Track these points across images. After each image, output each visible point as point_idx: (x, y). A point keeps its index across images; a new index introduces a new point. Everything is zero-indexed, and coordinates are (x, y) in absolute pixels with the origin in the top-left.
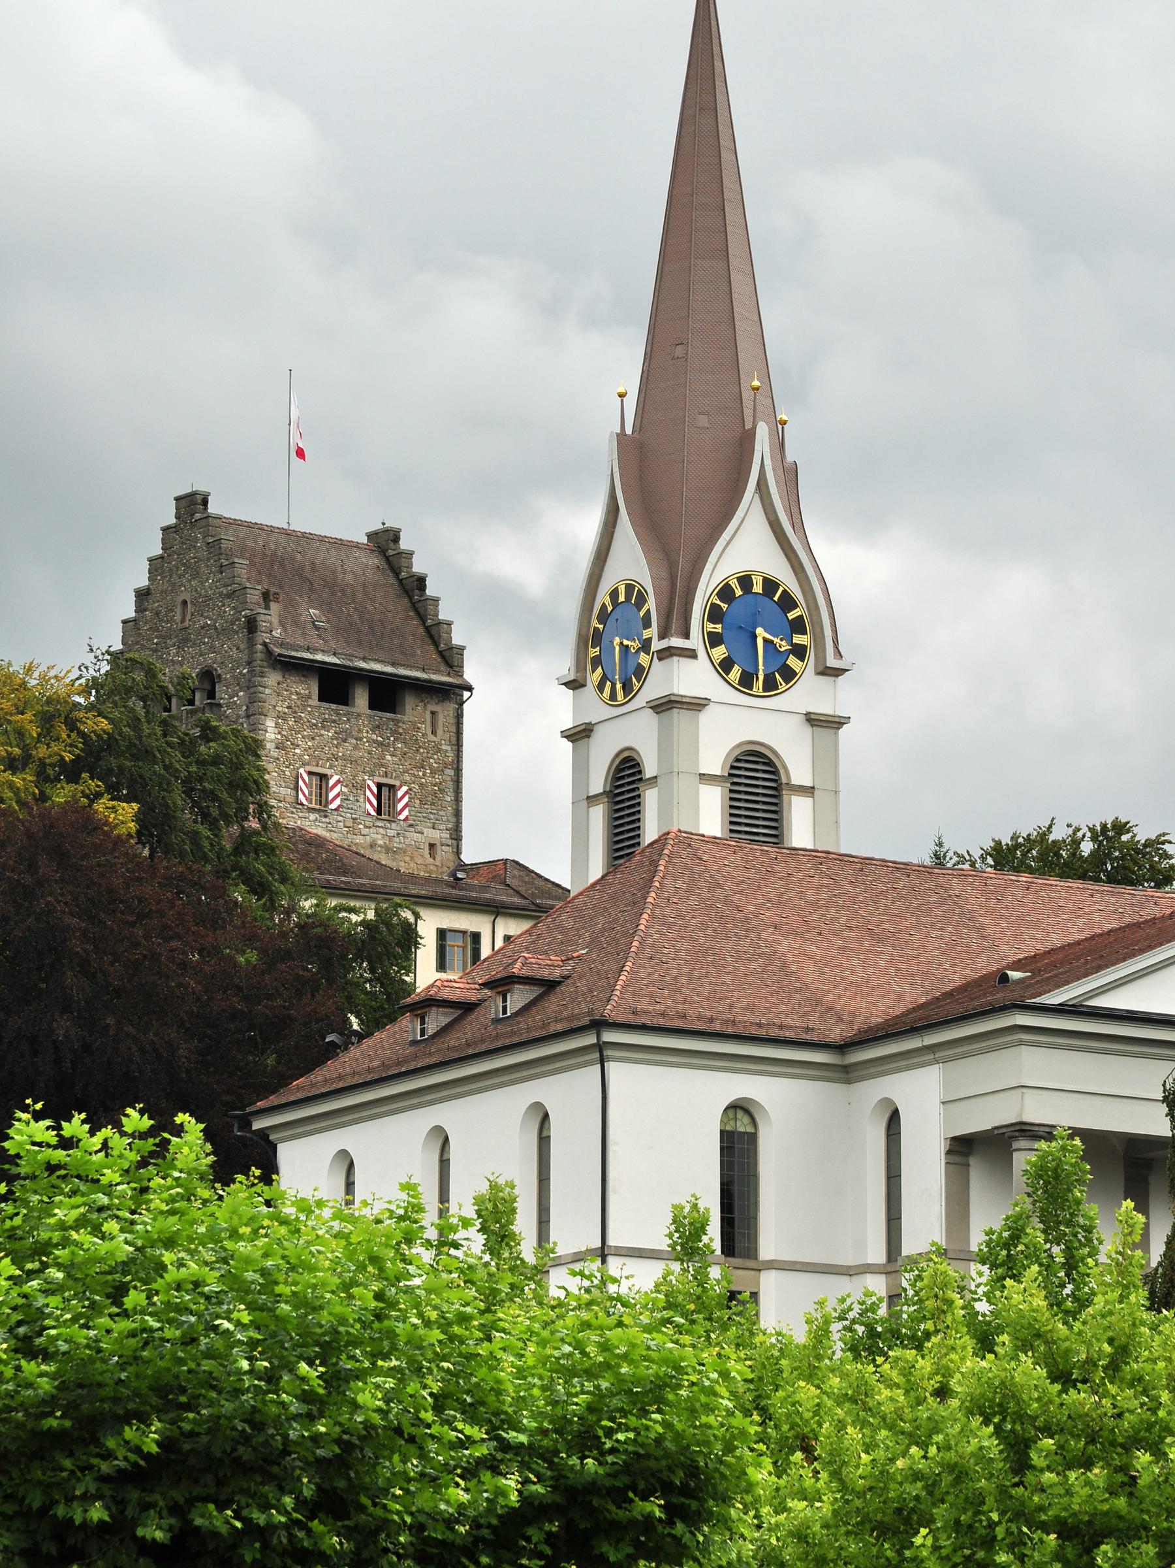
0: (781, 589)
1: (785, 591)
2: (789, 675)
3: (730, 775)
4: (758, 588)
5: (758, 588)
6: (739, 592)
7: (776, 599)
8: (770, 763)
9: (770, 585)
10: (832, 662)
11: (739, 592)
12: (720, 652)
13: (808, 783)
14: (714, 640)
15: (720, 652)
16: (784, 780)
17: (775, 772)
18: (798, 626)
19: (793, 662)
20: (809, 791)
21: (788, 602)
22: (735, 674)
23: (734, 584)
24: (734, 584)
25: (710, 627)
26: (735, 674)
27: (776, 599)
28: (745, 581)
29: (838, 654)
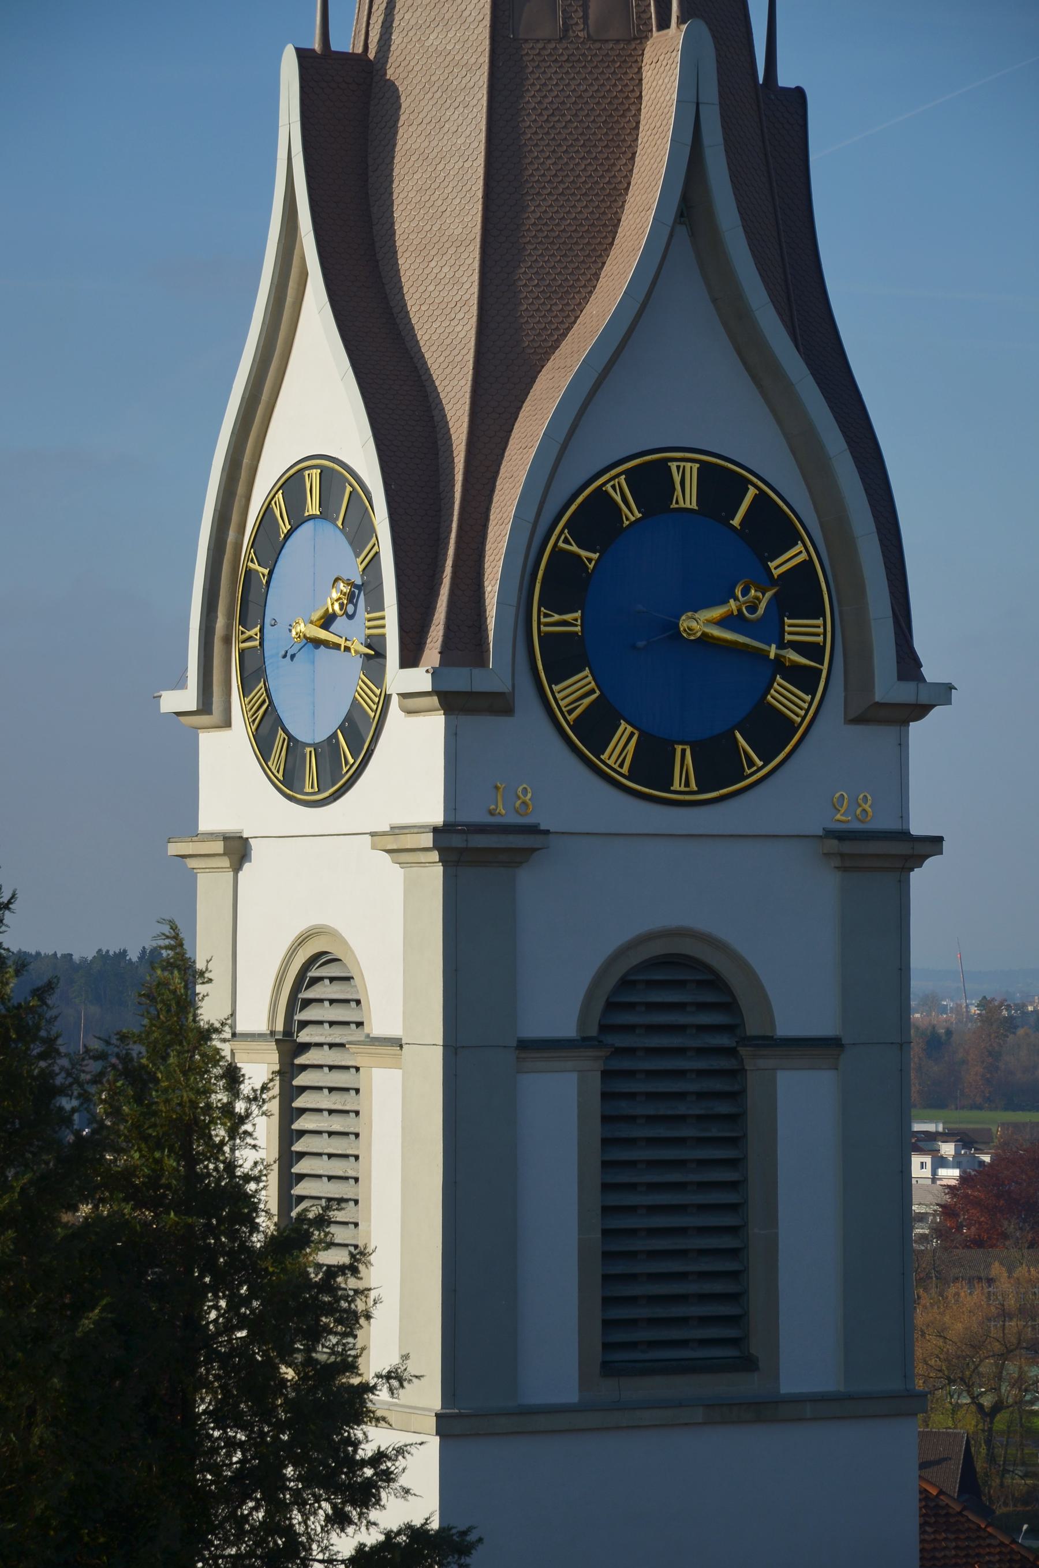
0: (752, 492)
1: (761, 498)
2: (774, 733)
3: (603, 1028)
4: (687, 498)
5: (687, 498)
6: (632, 514)
7: (736, 522)
8: (714, 981)
9: (721, 483)
10: (887, 687)
11: (632, 514)
12: (577, 691)
14: (561, 657)
15: (577, 691)
16: (753, 1029)
17: (731, 1006)
18: (799, 594)
19: (782, 695)
21: (772, 527)
22: (622, 745)
23: (618, 489)
24: (618, 489)
25: (550, 622)
26: (622, 745)
27: (736, 522)
28: (651, 480)
29: (909, 664)
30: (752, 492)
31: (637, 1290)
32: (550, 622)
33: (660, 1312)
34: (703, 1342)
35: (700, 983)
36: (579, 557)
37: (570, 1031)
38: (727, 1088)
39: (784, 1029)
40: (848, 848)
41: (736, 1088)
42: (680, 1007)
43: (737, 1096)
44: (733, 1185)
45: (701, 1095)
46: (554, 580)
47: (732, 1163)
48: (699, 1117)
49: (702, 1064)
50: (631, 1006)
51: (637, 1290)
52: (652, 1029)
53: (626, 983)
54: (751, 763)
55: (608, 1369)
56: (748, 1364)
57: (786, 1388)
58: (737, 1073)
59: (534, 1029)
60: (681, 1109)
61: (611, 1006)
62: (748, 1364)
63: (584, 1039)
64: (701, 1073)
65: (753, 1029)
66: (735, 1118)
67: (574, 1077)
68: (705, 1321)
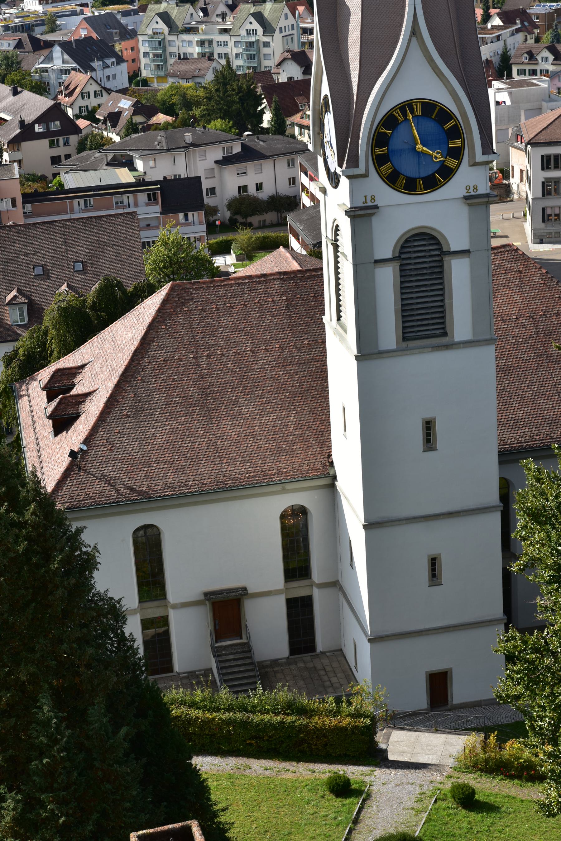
0: (438, 108)
3: (401, 253)
8: (434, 238)
13: (466, 247)
16: (445, 249)
17: (438, 243)
20: (466, 252)
27: (433, 117)
30: (438, 108)
31: (414, 318)
32: (378, 151)
33: (419, 323)
34: (433, 329)
35: (429, 238)
36: (386, 133)
37: (390, 256)
38: (438, 265)
39: (453, 249)
40: (469, 201)
41: (441, 264)
42: (424, 245)
43: (442, 266)
44: (441, 289)
45: (431, 267)
46: (379, 139)
47: (441, 284)
48: (430, 273)
49: (431, 259)
50: (409, 247)
51: (414, 318)
52: (415, 252)
53: (407, 241)
54: (440, 181)
55: (405, 339)
56: (445, 334)
57: (458, 337)
58: (441, 261)
59: (378, 257)
60: (425, 271)
61: (402, 247)
62: (445, 334)
63: (394, 257)
64: (430, 262)
65: (445, 249)
66: (442, 272)
67: (391, 268)
68: (434, 324)
